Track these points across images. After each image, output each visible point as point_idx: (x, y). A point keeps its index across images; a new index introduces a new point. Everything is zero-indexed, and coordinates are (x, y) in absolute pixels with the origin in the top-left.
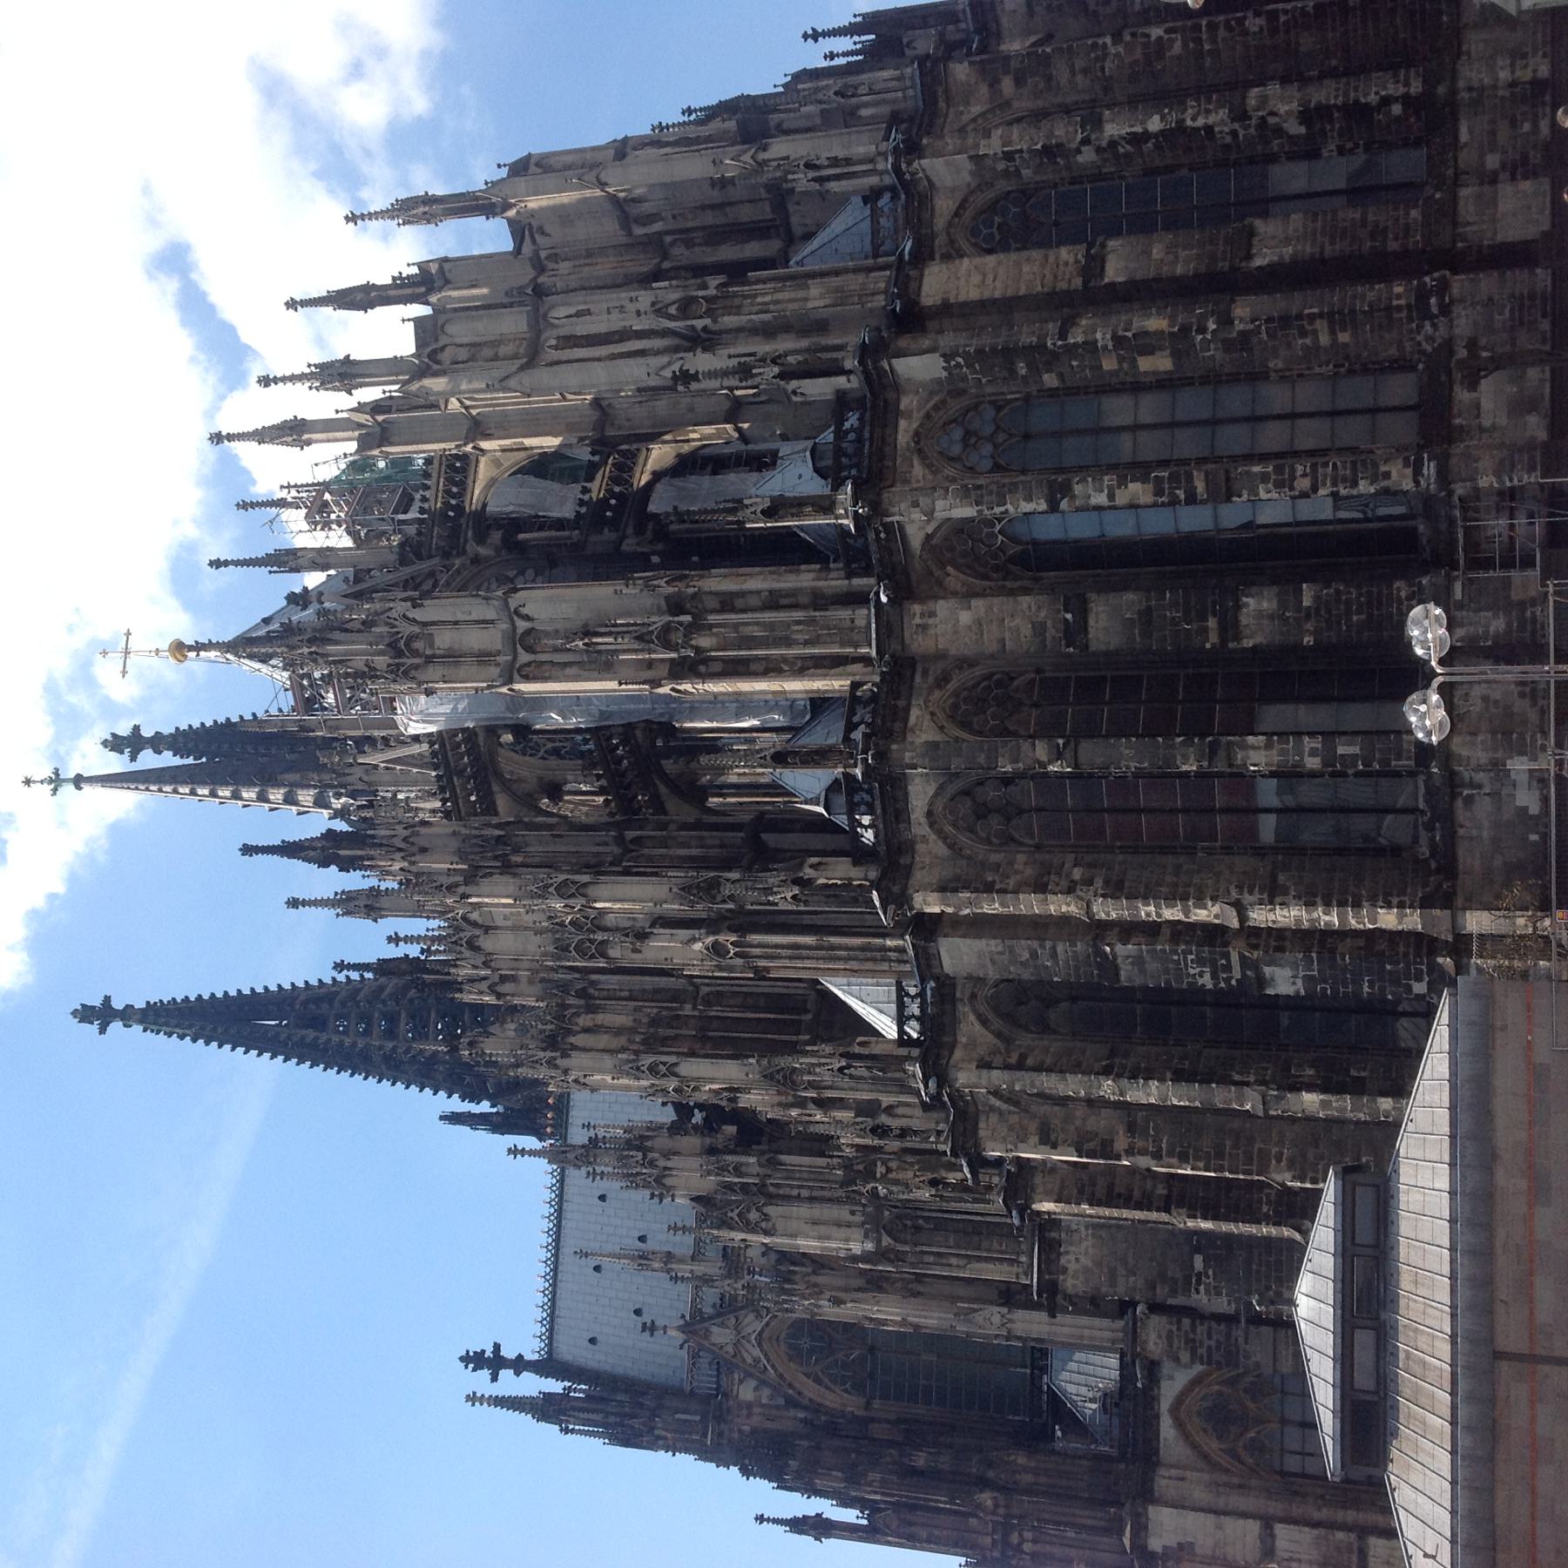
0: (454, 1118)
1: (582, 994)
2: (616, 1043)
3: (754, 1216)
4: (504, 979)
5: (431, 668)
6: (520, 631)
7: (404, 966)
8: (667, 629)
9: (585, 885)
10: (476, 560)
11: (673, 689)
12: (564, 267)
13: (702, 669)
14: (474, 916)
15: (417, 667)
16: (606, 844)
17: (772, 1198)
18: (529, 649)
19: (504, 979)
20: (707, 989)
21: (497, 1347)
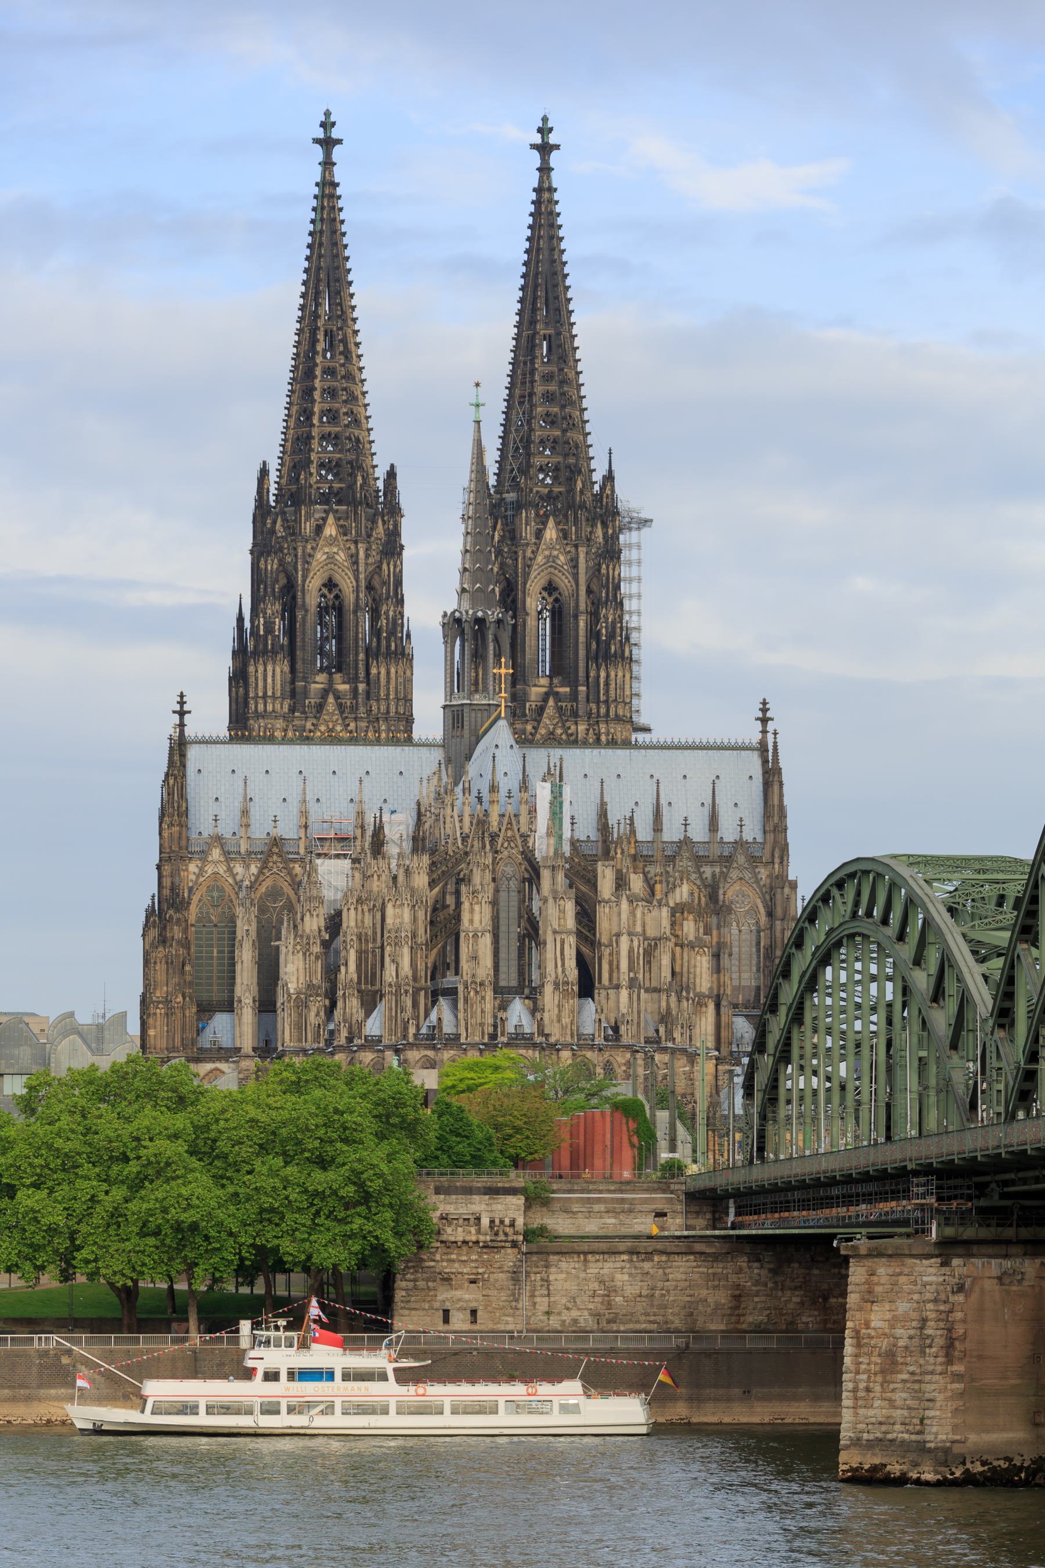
1: (374, 906)
3: (298, 947)
12: (607, 910)
17: (304, 954)
19: (379, 876)
21: (189, 712)
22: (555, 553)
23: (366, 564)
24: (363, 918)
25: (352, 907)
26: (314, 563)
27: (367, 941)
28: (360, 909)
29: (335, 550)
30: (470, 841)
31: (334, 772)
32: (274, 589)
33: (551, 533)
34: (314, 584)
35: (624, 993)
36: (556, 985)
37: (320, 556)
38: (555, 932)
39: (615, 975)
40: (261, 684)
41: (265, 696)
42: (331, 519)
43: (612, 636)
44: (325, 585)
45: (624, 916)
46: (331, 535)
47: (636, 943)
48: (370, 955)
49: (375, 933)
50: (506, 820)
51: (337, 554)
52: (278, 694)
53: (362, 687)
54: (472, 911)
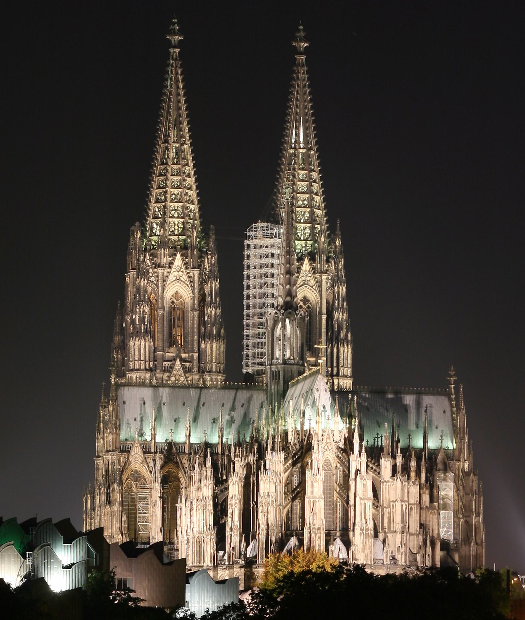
22: (308, 278)
32: (144, 297)
33: (306, 266)
35: (399, 536)
36: (362, 530)
37: (172, 278)
38: (361, 499)
39: (392, 525)
40: (137, 353)
41: (140, 360)
43: (340, 328)
45: (399, 490)
47: (404, 507)
52: (147, 359)
53: (196, 355)
54: (312, 486)
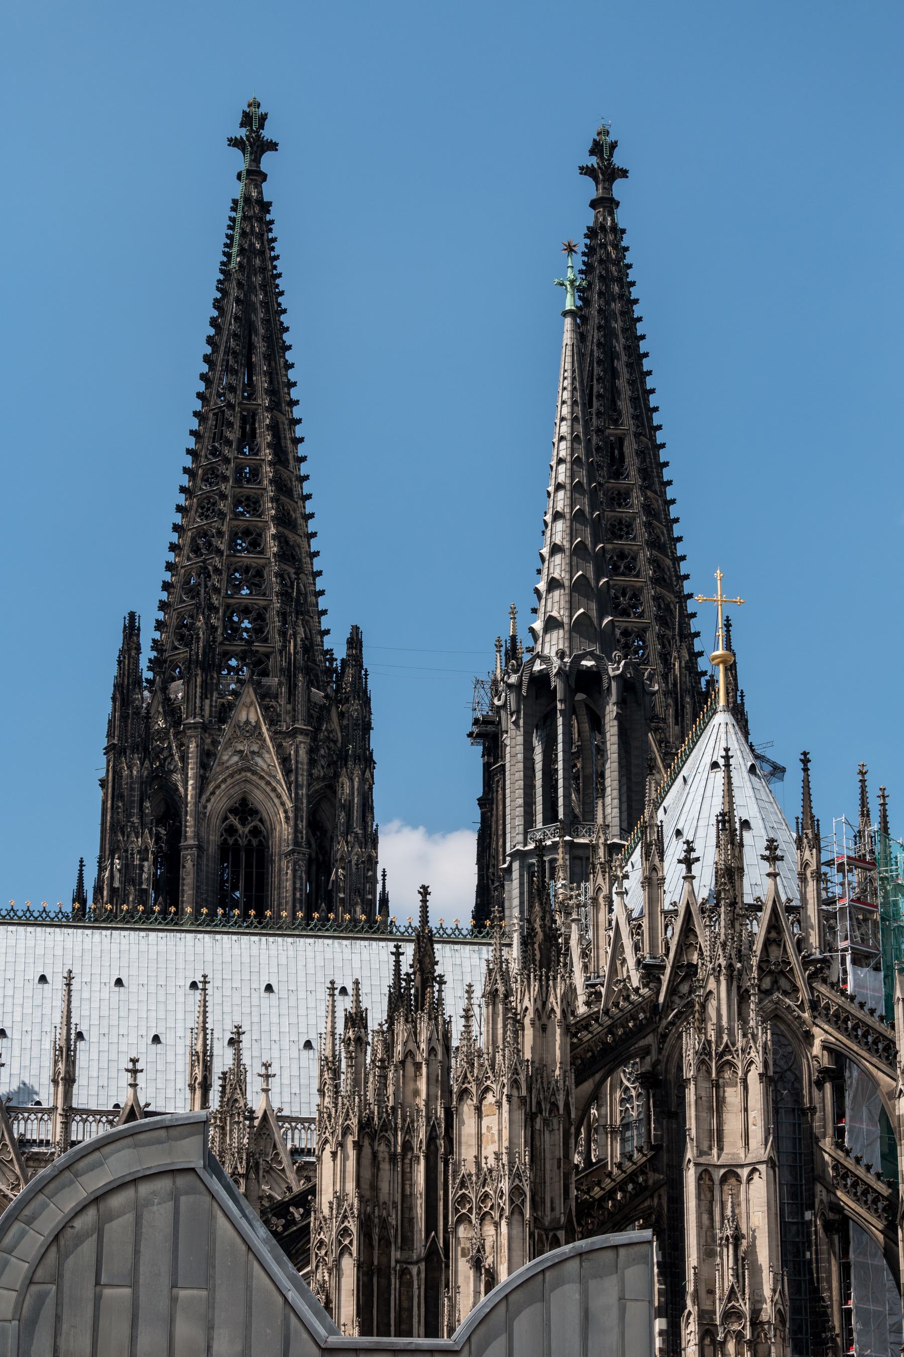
0: (131, 629)
2: (365, 1186)
4: (418, 1066)
5: (707, 1085)
6: (739, 1171)
7: (427, 960)
8: (739, 1315)
9: (522, 1214)
10: (809, 1037)
11: (690, 1313)
13: (707, 1341)
14: (490, 1099)
15: (709, 1072)
16: (553, 1209)
18: (724, 1179)
20: (414, 1270)
23: (310, 775)
24: (375, 1176)
25: (350, 1140)
26: (216, 768)
27: (385, 1243)
28: (367, 1150)
29: (255, 748)
30: (665, 978)
31: (269, 988)
34: (218, 804)
42: (249, 695)
44: (233, 811)
46: (247, 722)
48: (395, 1282)
49: (408, 1221)
50: (765, 916)
51: (259, 754)
